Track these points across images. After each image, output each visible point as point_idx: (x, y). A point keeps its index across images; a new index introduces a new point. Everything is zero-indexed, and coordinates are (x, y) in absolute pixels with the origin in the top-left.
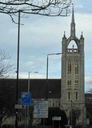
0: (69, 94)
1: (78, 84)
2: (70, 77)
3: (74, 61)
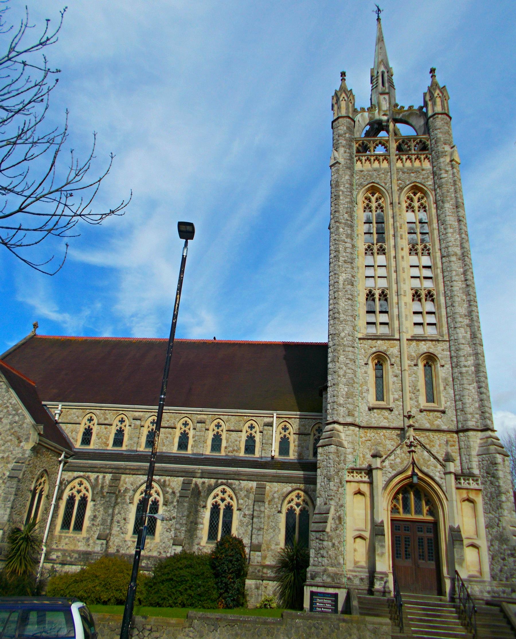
0: (380, 360)
1: (429, 306)
2: (382, 272)
3: (401, 189)
